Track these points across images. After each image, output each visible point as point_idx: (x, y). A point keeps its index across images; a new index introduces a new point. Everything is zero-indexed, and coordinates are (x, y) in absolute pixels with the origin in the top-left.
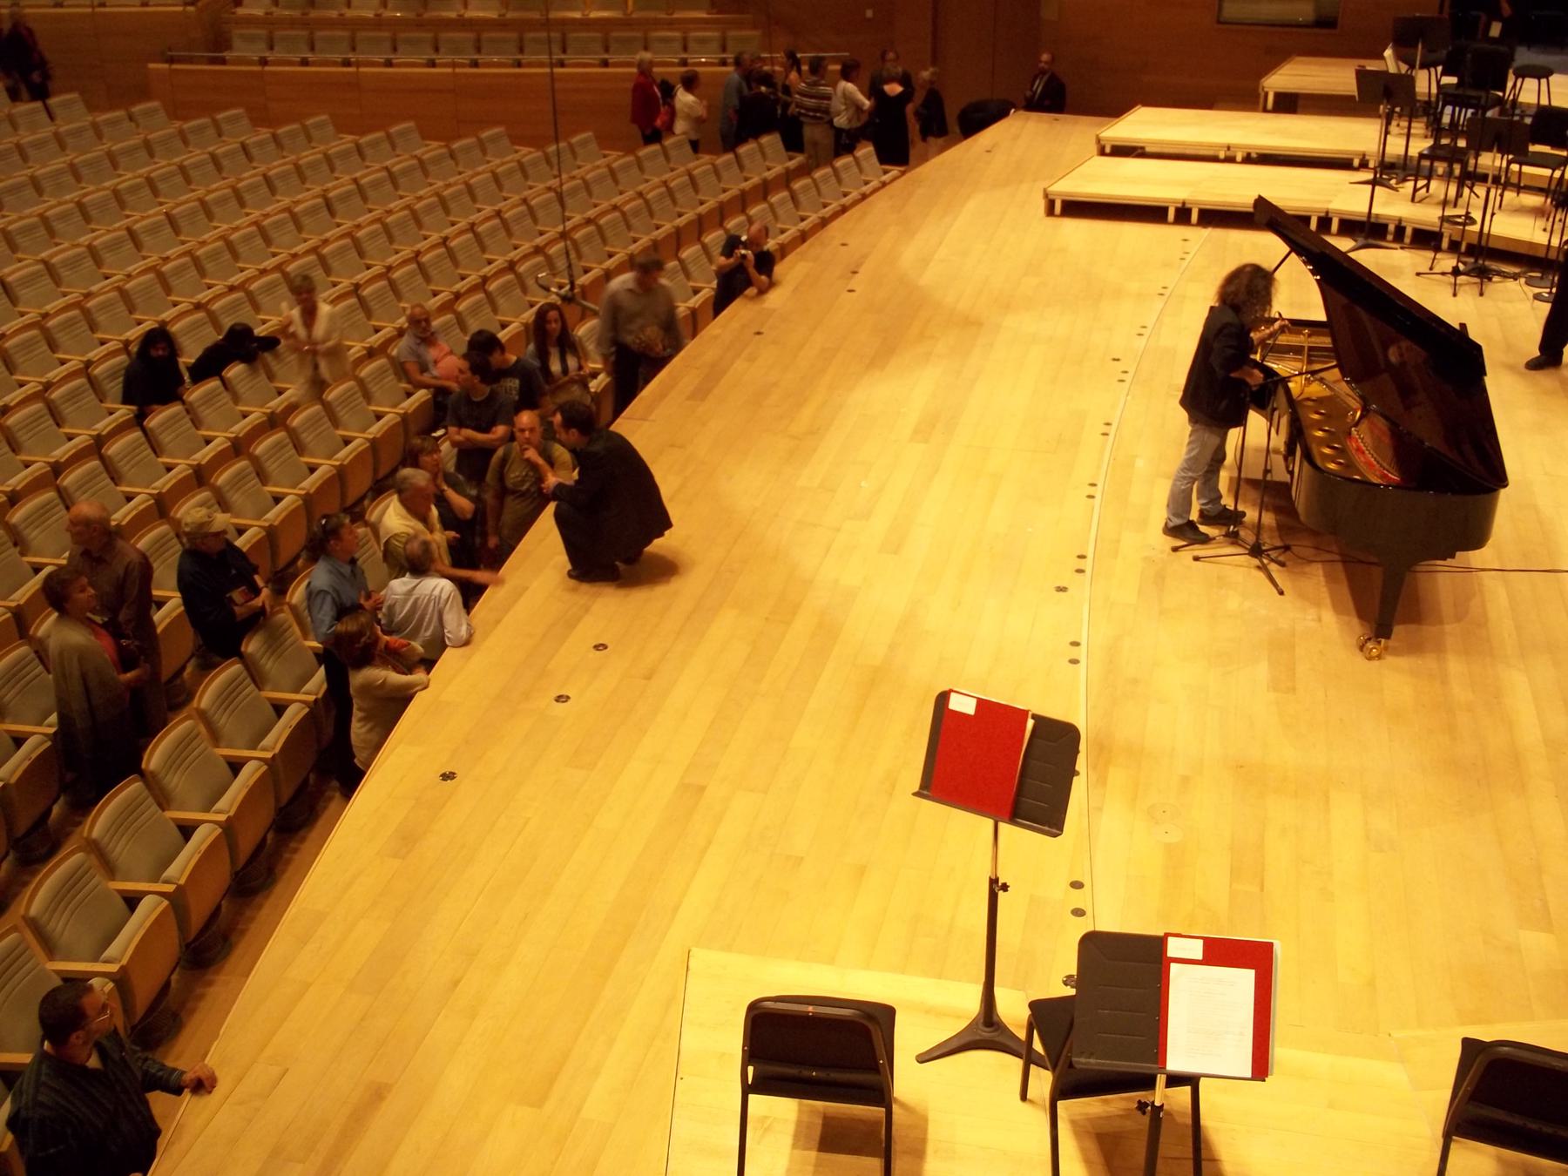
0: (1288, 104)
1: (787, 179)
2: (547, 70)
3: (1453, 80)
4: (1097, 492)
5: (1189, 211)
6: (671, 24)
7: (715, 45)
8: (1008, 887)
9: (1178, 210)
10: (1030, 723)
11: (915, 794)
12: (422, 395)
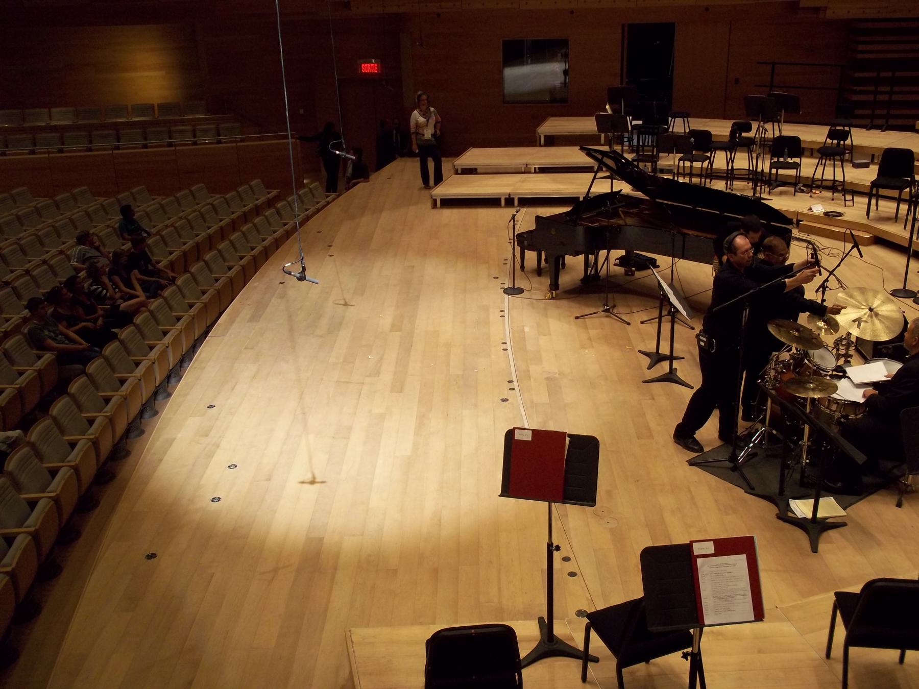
0: (552, 141)
1: (270, 203)
2: (111, 152)
3: (640, 122)
4: (508, 346)
6: (183, 122)
8: (560, 550)
9: (506, 199)
10: (568, 439)
11: (499, 496)
12: (48, 357)
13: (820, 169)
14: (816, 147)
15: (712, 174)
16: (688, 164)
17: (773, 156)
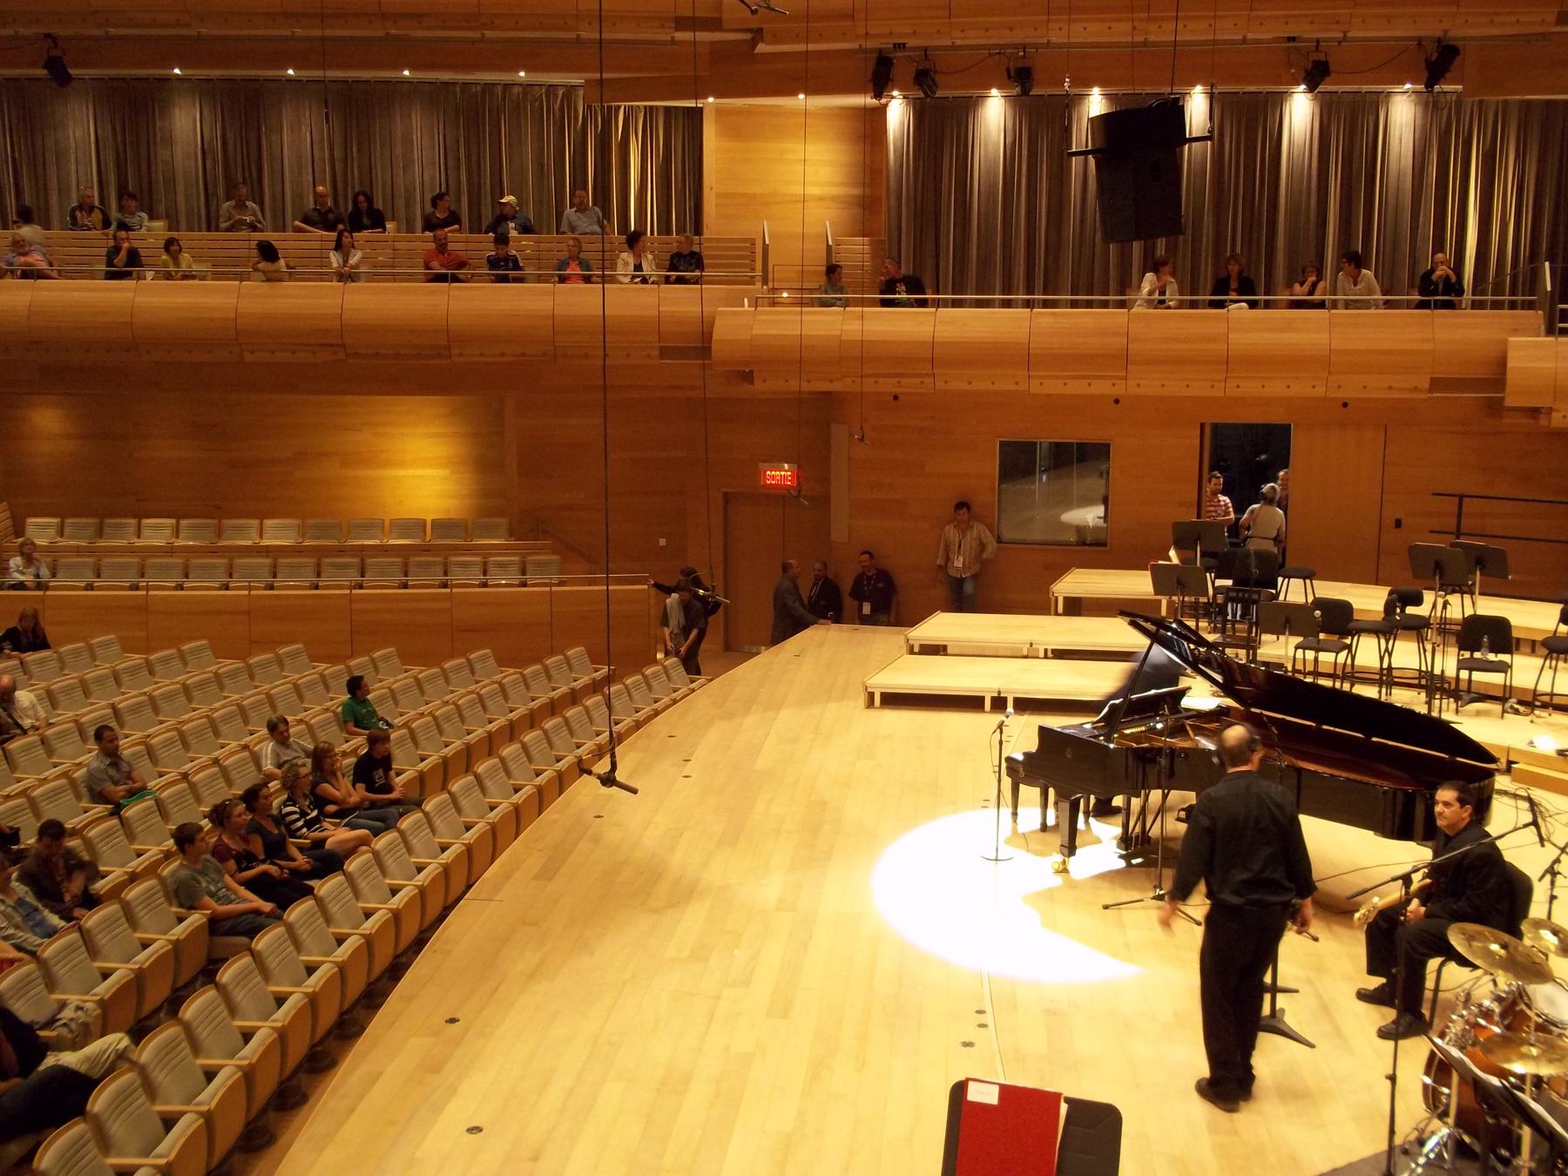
0: (1075, 607)
1: (595, 687)
2: (348, 592)
3: (1229, 582)
5: (1005, 700)
6: (468, 550)
7: (515, 568)
9: (993, 698)
10: (1064, 1108)
13: (1548, 674)
14: (1540, 638)
15: (1354, 675)
16: (1310, 655)
17: (1462, 647)
